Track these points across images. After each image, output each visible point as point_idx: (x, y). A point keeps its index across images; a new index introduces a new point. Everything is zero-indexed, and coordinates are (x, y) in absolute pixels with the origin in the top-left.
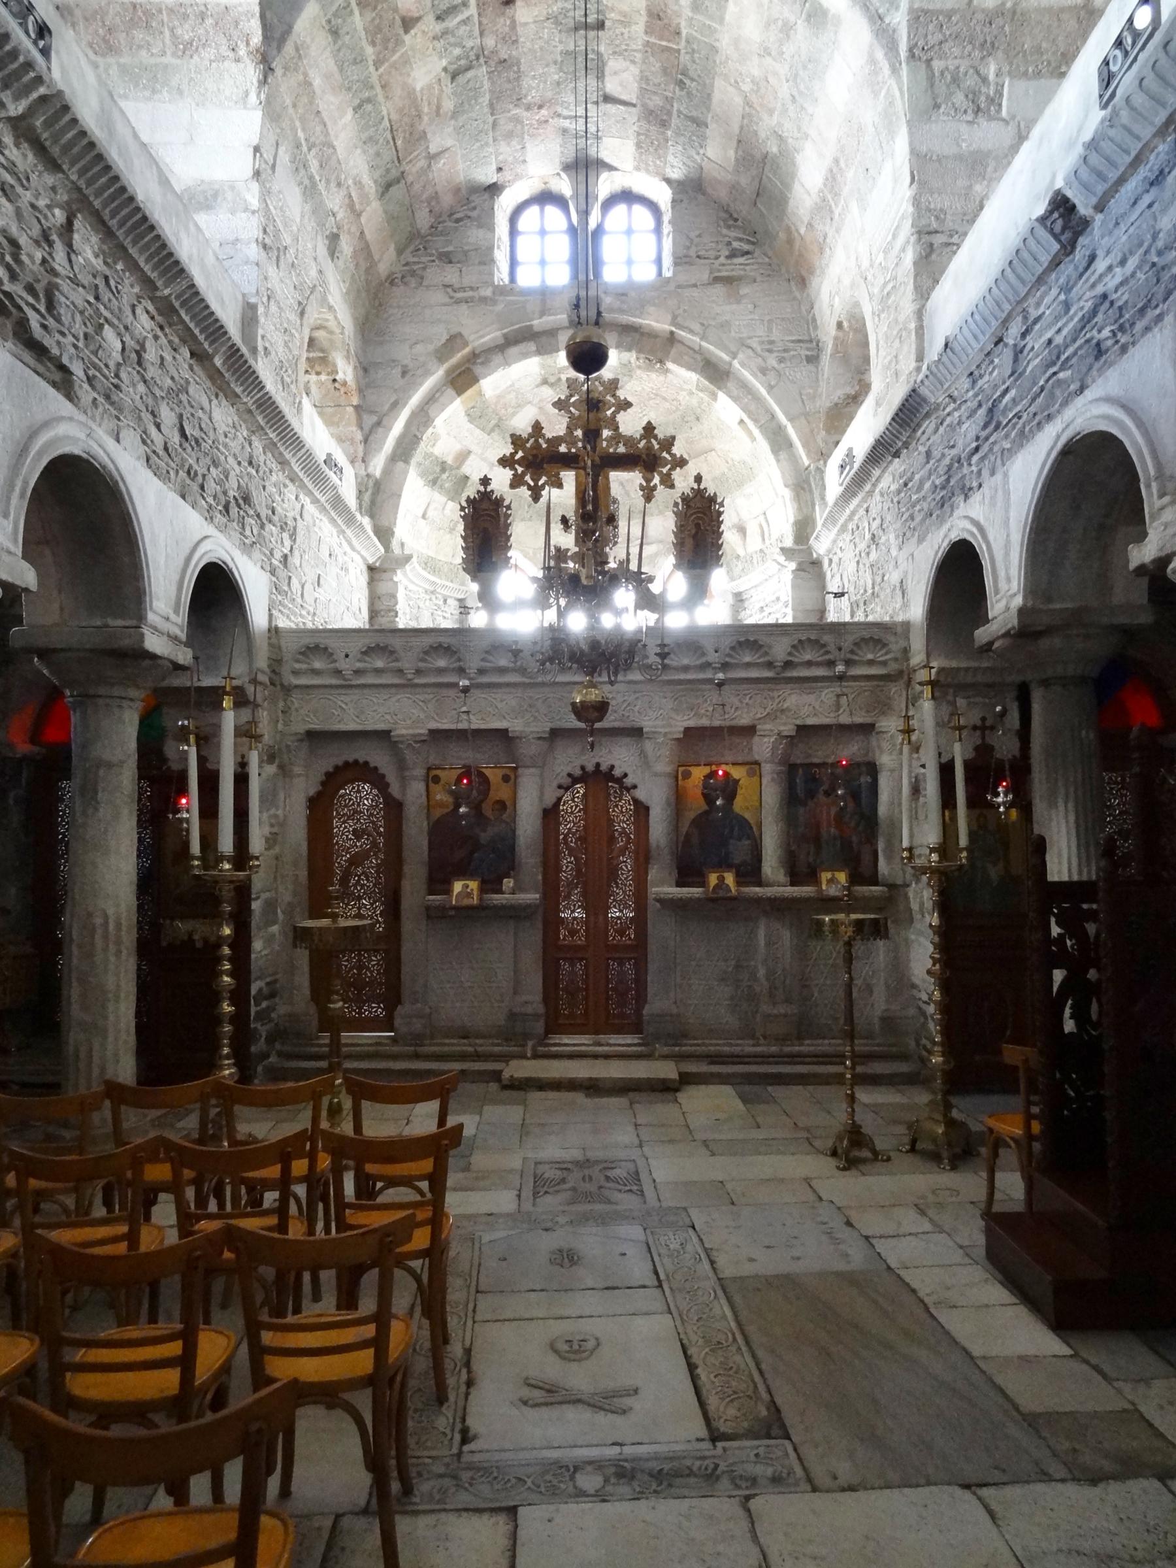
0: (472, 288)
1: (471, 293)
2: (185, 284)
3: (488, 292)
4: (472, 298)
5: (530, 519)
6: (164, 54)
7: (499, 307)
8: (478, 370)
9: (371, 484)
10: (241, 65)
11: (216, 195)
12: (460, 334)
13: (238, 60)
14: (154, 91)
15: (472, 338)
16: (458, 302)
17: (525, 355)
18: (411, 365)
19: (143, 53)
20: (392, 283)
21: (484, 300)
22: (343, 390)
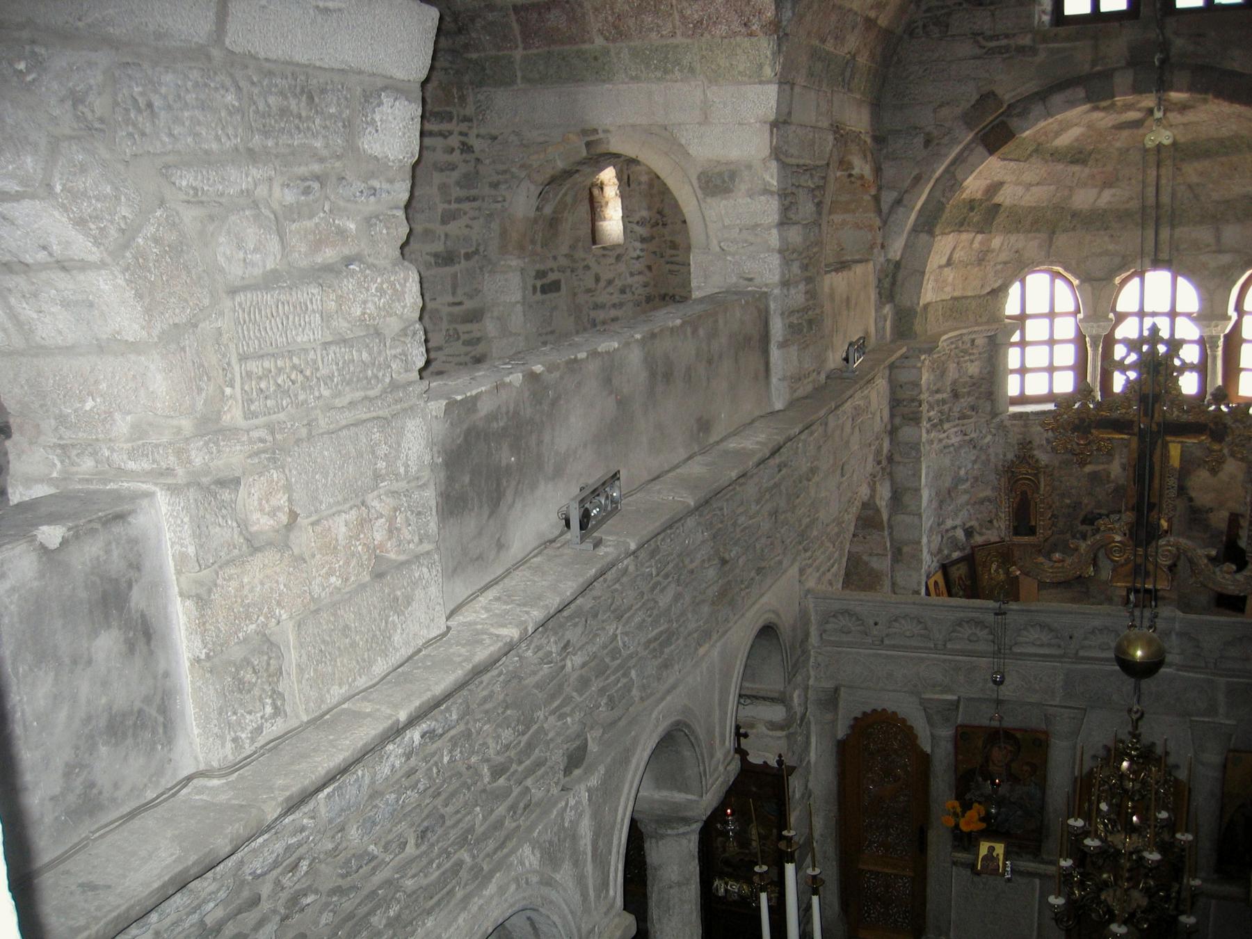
0: (1007, 36)
1: (1004, 42)
2: (747, 684)
3: (1027, 40)
4: (1007, 49)
5: (1074, 229)
6: (674, 35)
7: (1041, 57)
8: (1014, 123)
9: (891, 266)
10: (754, 39)
11: (733, 175)
12: (992, 94)
13: (751, 35)
14: (666, 72)
15: (1007, 97)
16: (992, 52)
17: (1072, 104)
18: (935, 133)
19: (653, 35)
20: (911, 34)
21: (1021, 50)
22: (859, 182)
